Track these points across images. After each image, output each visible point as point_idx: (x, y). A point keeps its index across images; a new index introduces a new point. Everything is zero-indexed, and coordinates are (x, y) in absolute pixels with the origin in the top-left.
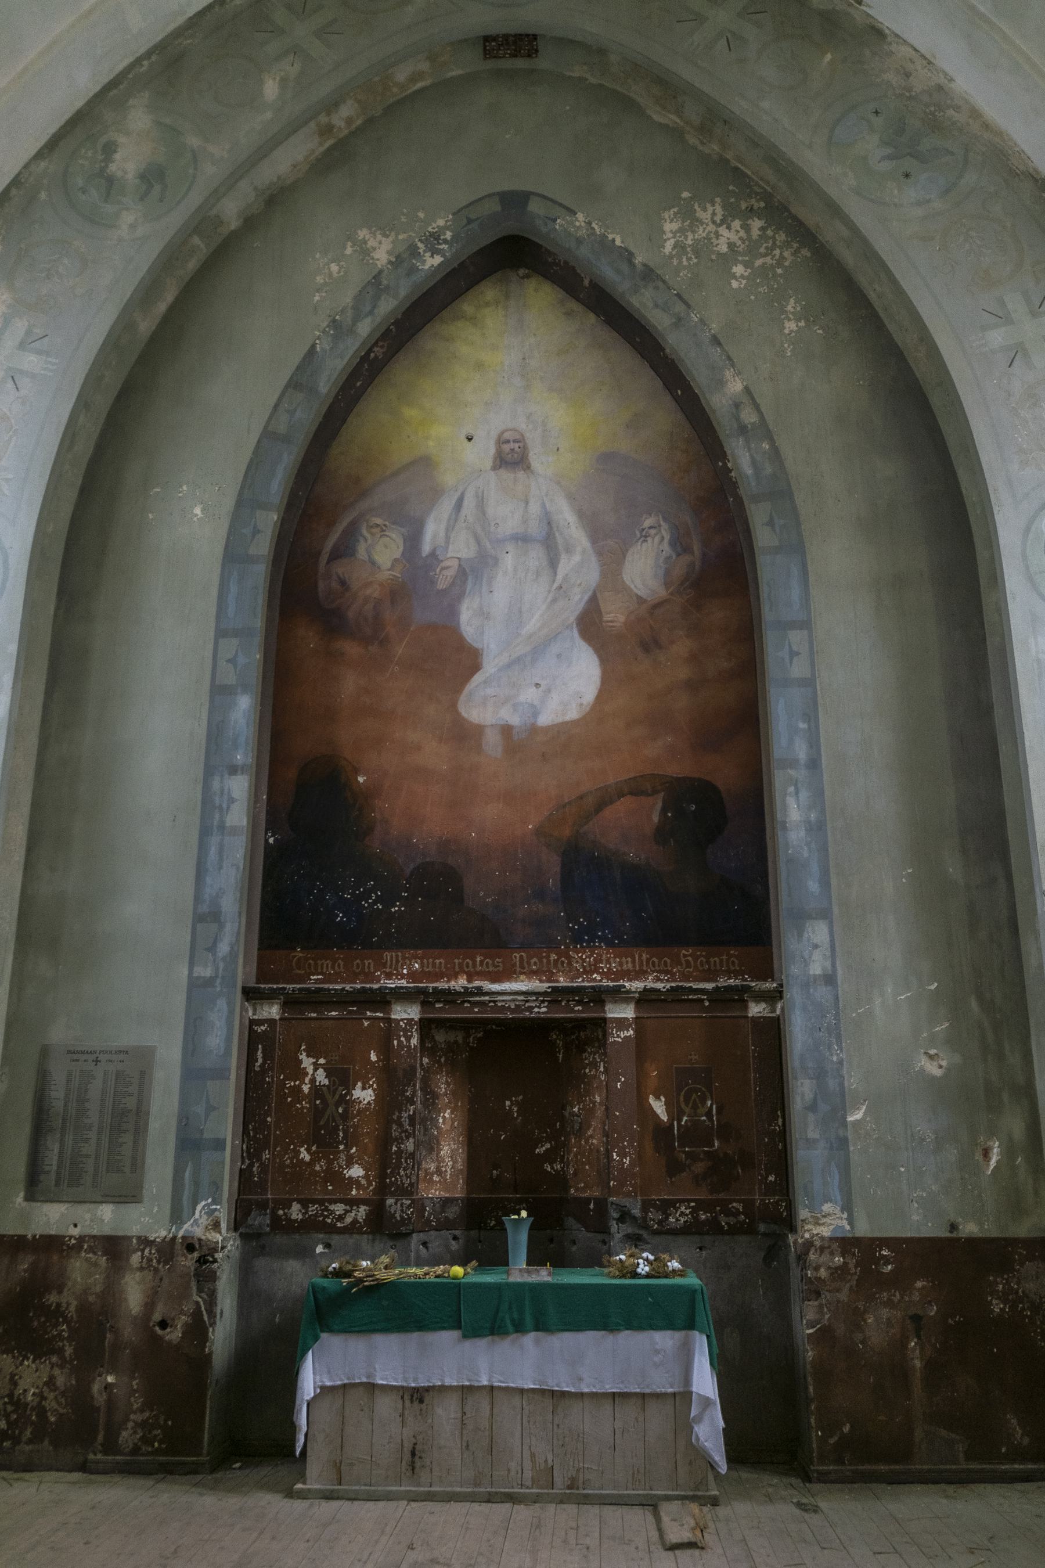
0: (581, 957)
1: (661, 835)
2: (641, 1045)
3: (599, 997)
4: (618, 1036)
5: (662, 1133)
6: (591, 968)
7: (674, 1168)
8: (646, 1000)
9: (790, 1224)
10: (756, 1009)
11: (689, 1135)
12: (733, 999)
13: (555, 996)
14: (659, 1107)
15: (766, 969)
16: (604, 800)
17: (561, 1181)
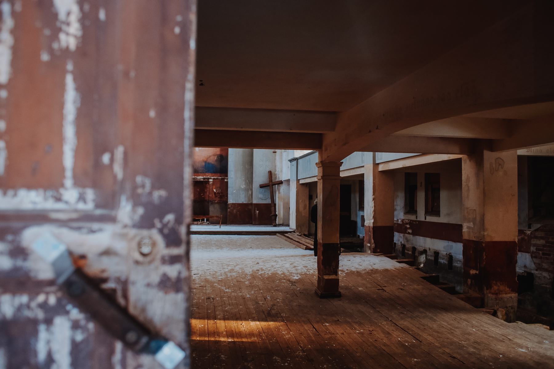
0: (207, 174)
1: (216, 161)
2: (213, 184)
3: (209, 179)
4: (211, 183)
5: (215, 193)
6: (208, 176)
7: (216, 197)
8: (214, 179)
9: (227, 202)
10: (226, 180)
11: (218, 193)
12: (224, 179)
13: (204, 179)
14: (215, 190)
15: (227, 176)
16: (210, 157)
17: (204, 198)
